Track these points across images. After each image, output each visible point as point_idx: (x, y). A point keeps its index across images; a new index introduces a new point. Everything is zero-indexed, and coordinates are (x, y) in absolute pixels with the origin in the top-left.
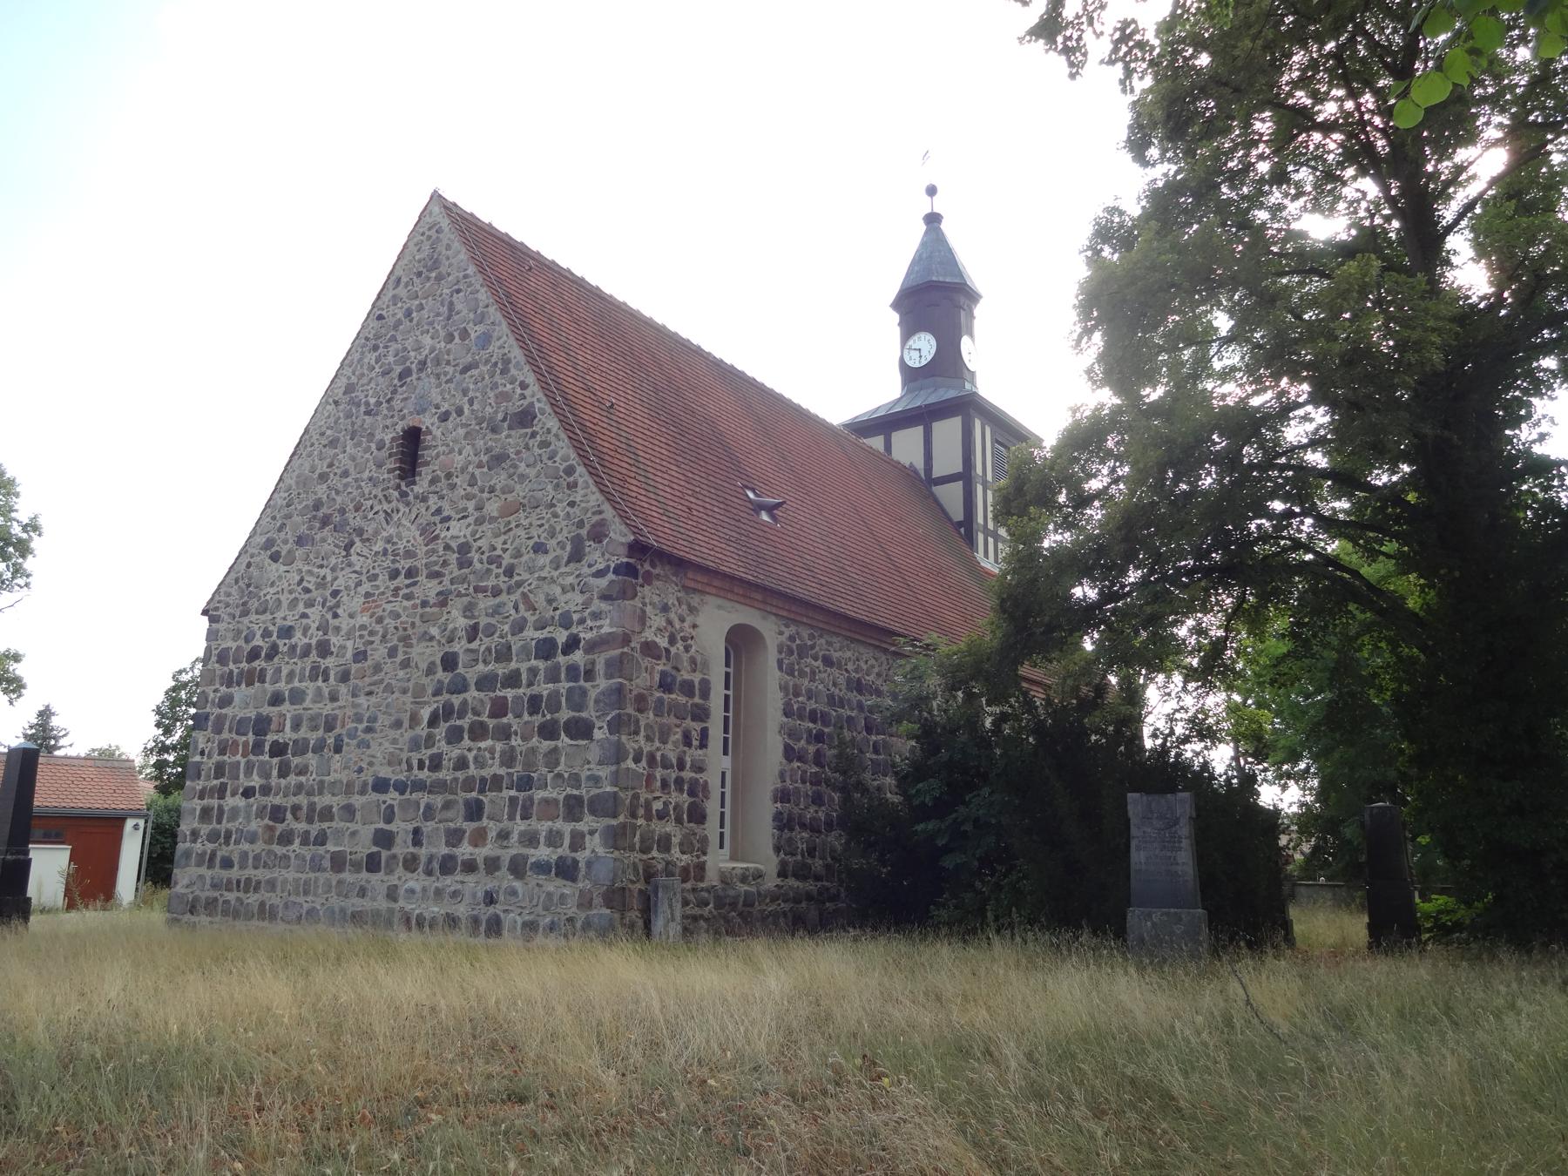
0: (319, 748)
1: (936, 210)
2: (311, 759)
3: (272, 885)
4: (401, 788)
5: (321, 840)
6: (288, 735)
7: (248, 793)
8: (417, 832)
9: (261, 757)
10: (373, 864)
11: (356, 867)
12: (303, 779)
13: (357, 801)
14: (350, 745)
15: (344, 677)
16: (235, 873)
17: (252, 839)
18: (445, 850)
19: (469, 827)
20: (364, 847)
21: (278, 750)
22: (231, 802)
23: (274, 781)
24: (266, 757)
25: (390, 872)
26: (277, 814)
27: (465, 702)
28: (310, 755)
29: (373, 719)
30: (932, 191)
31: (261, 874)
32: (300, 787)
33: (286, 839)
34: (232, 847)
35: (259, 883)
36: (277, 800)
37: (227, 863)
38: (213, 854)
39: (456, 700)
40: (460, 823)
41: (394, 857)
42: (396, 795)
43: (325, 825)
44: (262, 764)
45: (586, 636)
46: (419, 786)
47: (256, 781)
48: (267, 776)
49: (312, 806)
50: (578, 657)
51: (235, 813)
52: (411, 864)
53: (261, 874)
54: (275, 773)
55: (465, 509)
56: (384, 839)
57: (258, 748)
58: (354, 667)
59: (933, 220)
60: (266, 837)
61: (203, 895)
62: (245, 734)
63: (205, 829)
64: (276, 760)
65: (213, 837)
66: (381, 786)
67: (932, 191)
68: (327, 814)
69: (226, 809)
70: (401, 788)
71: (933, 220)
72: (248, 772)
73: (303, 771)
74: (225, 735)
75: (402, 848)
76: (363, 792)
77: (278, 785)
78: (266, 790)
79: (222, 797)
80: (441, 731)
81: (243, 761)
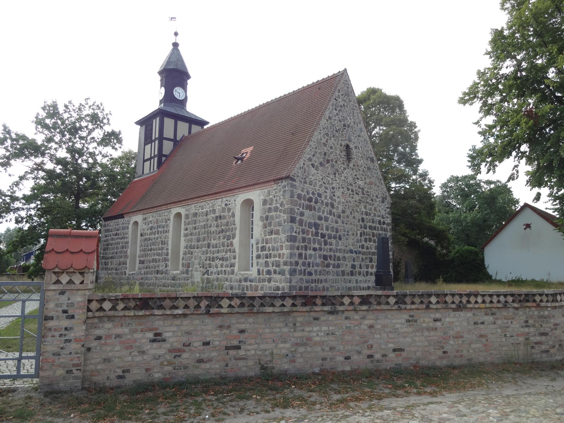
0: (335, 238)
1: (177, 42)
2: (333, 241)
3: (326, 281)
4: (356, 253)
5: (338, 266)
6: (325, 231)
7: (315, 249)
8: (360, 265)
9: (317, 238)
10: (352, 274)
11: (348, 274)
12: (331, 247)
13: (347, 255)
14: (344, 239)
15: (339, 217)
16: (314, 277)
17: (317, 265)
18: (366, 270)
19: (370, 264)
20: (349, 269)
21: (323, 236)
22: (309, 252)
23: (323, 246)
24: (319, 238)
25: (356, 276)
26: (325, 257)
27: (367, 232)
28: (332, 239)
29: (348, 232)
30: (176, 34)
31: (323, 277)
32: (331, 250)
33: (328, 266)
34: (311, 268)
35: (321, 280)
36: (325, 253)
37: (310, 274)
38: (305, 270)
39: (365, 231)
40: (368, 263)
41: (356, 272)
42: (354, 254)
43: (339, 262)
44: (319, 240)
45: (386, 222)
46: (360, 252)
47: (317, 246)
48: (321, 245)
49: (335, 256)
50: (385, 226)
51: (311, 256)
52: (360, 273)
53: (323, 277)
54: (323, 244)
55: (362, 178)
56: (353, 267)
57: (317, 234)
58: (342, 215)
59: (175, 45)
60: (323, 265)
61: (303, 285)
62: (312, 228)
63: (301, 262)
64: (322, 239)
65: (304, 264)
66: (351, 251)
67: (176, 34)
68: (339, 259)
69: (307, 254)
70: (356, 253)
71: (175, 45)
72: (314, 243)
73: (331, 244)
74: (304, 227)
75: (357, 269)
76: (347, 253)
77: (324, 248)
78: (320, 249)
79: (306, 250)
80: (363, 238)
81: (312, 238)
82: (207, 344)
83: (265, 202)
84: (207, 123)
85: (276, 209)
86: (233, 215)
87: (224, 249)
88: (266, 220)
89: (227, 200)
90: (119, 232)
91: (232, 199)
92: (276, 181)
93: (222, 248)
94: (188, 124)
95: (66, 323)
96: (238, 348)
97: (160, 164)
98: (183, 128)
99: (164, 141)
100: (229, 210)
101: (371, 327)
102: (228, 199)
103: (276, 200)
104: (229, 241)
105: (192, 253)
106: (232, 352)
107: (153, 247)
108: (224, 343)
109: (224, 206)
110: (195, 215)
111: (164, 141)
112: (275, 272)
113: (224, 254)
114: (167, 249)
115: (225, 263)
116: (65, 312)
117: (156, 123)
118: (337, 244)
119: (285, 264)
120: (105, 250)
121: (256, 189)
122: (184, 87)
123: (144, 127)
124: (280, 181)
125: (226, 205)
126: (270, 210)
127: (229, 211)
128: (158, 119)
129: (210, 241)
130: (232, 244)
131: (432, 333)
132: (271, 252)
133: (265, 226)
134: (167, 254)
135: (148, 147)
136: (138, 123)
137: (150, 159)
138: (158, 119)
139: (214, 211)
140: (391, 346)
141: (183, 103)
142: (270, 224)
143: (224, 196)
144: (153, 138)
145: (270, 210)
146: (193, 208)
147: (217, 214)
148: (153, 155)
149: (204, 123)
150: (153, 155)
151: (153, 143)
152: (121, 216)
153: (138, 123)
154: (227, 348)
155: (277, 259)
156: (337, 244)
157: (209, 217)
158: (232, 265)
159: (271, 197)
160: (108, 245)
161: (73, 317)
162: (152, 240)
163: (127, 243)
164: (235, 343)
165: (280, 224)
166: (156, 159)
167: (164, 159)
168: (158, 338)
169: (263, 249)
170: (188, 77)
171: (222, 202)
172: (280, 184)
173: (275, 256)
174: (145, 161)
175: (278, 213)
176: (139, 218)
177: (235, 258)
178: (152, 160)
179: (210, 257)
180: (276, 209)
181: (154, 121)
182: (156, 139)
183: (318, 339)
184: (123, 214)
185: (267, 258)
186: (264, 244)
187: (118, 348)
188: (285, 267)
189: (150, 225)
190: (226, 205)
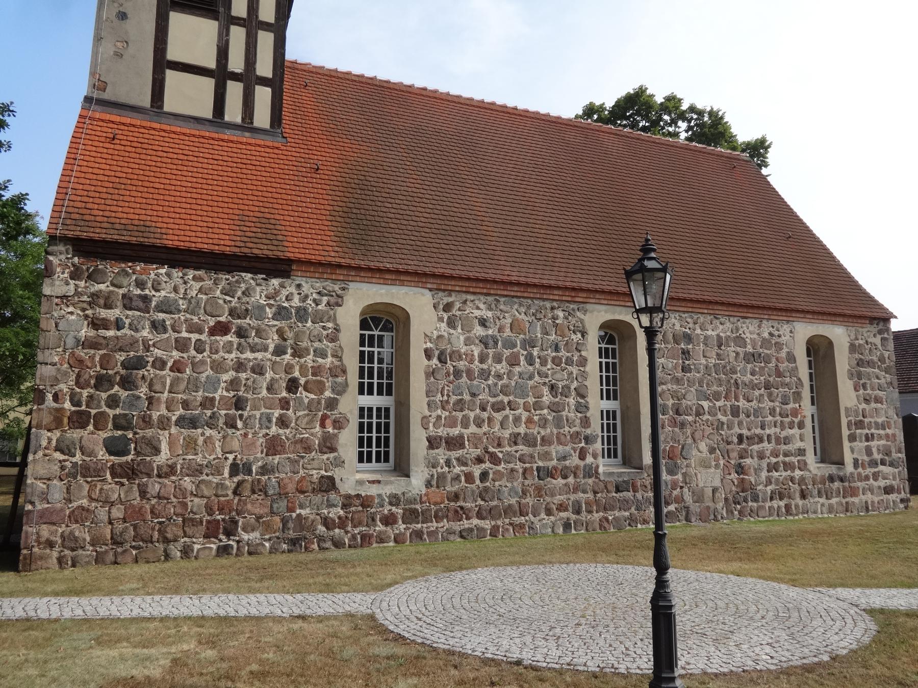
86: (791, 358)
87: (775, 423)
89: (773, 327)
91: (785, 329)
93: (770, 418)
100: (779, 347)
109: (766, 335)
112: (883, 463)
113: (778, 430)
115: (783, 447)
121: (835, 323)
124: (876, 322)
127: (779, 347)
129: (737, 399)
132: (873, 431)
139: (740, 341)
143: (766, 317)
147: (749, 349)
155: (883, 442)
157: (731, 350)
158: (801, 452)
169: (860, 424)
171: (759, 326)
172: (875, 325)
173: (880, 437)
184: (289, 262)
185: (867, 440)
186: (861, 418)
189: (479, 331)
190: (771, 334)
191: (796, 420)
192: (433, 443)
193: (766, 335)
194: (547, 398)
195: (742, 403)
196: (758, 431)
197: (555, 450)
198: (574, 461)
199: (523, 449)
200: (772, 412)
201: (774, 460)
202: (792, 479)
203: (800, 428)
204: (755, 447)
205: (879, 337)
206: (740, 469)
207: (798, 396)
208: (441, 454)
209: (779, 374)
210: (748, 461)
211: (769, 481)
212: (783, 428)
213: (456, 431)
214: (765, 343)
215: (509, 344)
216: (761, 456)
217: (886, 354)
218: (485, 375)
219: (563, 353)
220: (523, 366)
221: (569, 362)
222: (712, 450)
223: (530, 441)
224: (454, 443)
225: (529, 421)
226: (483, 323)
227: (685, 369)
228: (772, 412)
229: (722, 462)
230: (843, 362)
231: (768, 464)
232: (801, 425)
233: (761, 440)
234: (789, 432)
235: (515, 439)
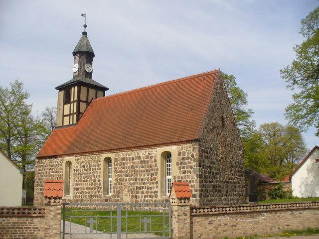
7: (210, 182)
30: (85, 26)
47: (211, 180)
56: (227, 191)
59: (85, 34)
67: (85, 26)
71: (85, 34)
82: (226, 224)
83: (180, 154)
84: (107, 89)
85: (188, 158)
86: (155, 161)
88: (180, 164)
90: (53, 167)
92: (188, 142)
94: (95, 91)
95: (184, 217)
96: (236, 226)
97: (78, 119)
98: (92, 92)
99: (81, 103)
100: (152, 157)
101: (279, 216)
102: (151, 150)
103: (188, 153)
104: (153, 177)
105: (122, 184)
106: (234, 228)
107: (86, 179)
108: (231, 224)
109: (147, 154)
110: (124, 159)
111: (81, 103)
114: (99, 181)
116: (184, 213)
117: (74, 91)
118: (220, 178)
119: (196, 191)
120: (39, 180)
122: (91, 64)
123: (62, 93)
125: (149, 154)
126: (183, 159)
128: (76, 88)
130: (155, 179)
131: (299, 219)
133: (180, 168)
134: (100, 184)
135: (67, 106)
136: (57, 88)
137: (69, 115)
138: (76, 88)
139: (139, 158)
140: (286, 224)
141: (89, 75)
142: (184, 168)
144: (72, 100)
145: (183, 159)
146: (121, 154)
147: (142, 160)
148: (72, 112)
149: (104, 89)
150: (72, 112)
151: (72, 104)
152: (56, 157)
153: (57, 88)
154: (232, 226)
156: (220, 178)
158: (156, 192)
159: (184, 151)
160: (42, 176)
161: (186, 215)
162: (85, 174)
163: (63, 175)
164: (235, 224)
165: (191, 167)
166: (75, 116)
167: (81, 115)
168: (210, 223)
170: (94, 56)
174: (64, 116)
175: (190, 161)
176: (72, 159)
177: (157, 187)
178: (71, 116)
179: (137, 187)
180: (188, 158)
181: (73, 89)
182: (74, 101)
183: (261, 222)
184: (57, 156)
187: (198, 227)
188: (196, 193)
189: (83, 164)
190: (149, 154)
191: (155, 182)
192: (75, 189)
193: (147, 154)
194: (93, 178)
195: (139, 177)
196: (142, 185)
197: (94, 191)
198: (97, 194)
199: (88, 191)
200: (148, 179)
201: (146, 194)
202: (152, 200)
203: (156, 184)
204: (141, 190)
205: (192, 147)
206: (136, 197)
207: (156, 173)
208: (76, 191)
209: (151, 166)
210: (139, 195)
211: (144, 201)
212: (150, 184)
213: (77, 187)
214: (147, 157)
215: (87, 167)
216: (143, 193)
217: (195, 154)
218: (83, 174)
219: (97, 167)
220: (89, 171)
221: (98, 169)
222: (128, 191)
223: (89, 189)
224: (77, 189)
225: (90, 184)
226: (83, 162)
227: (124, 168)
228: (148, 179)
229: (131, 195)
230: (175, 158)
231: (145, 196)
232: (157, 183)
233: (143, 188)
234: (152, 185)
235: (87, 188)
